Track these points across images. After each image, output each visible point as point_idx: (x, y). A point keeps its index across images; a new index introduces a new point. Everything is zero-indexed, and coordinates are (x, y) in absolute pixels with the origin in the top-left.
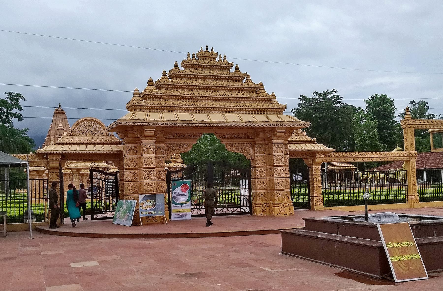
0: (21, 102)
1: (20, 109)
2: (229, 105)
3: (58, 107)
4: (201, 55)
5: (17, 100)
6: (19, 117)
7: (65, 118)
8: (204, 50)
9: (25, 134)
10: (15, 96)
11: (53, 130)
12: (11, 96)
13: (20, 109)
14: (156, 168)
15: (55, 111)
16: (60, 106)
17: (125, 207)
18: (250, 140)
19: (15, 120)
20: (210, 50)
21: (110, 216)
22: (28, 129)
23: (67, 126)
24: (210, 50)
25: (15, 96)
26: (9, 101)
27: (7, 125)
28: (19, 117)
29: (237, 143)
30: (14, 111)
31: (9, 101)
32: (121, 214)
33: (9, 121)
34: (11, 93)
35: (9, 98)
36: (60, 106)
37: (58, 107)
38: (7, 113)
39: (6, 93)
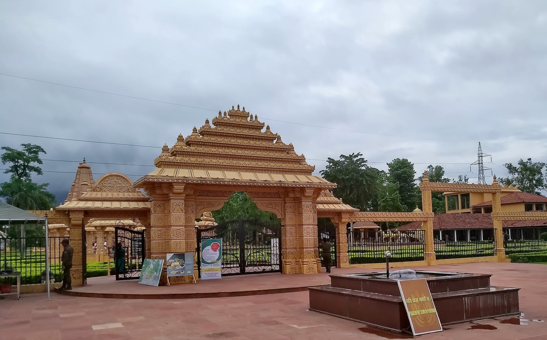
0: (41, 155)
1: (40, 162)
2: (260, 164)
4: (233, 114)
5: (36, 152)
6: (38, 171)
7: (90, 174)
8: (236, 109)
10: (33, 148)
11: (76, 185)
13: (40, 162)
14: (185, 226)
15: (79, 165)
16: (84, 161)
17: (152, 266)
18: (280, 199)
19: (33, 175)
20: (241, 110)
21: (136, 276)
22: (48, 184)
24: (241, 110)
25: (33, 148)
26: (27, 154)
27: (23, 179)
28: (38, 171)
29: (268, 202)
30: (32, 164)
31: (27, 154)
32: (147, 273)
33: (26, 175)
35: (27, 150)
36: (84, 161)
38: (24, 166)
39: (23, 145)
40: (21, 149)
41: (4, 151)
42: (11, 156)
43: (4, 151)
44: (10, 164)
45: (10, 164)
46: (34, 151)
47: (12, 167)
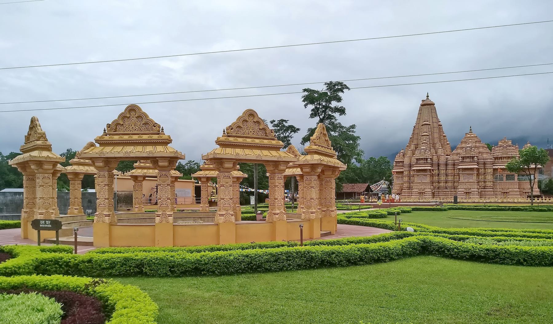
3: (425, 98)
6: (342, 111)
9: (353, 132)
12: (331, 86)
15: (421, 102)
16: (428, 96)
19: (336, 115)
22: (354, 125)
23: (435, 120)
25: (334, 86)
28: (342, 111)
30: (334, 104)
31: (329, 94)
33: (330, 117)
34: (331, 83)
36: (428, 96)
37: (425, 98)
39: (326, 84)
40: (322, 88)
41: (306, 93)
42: (311, 97)
43: (306, 93)
44: (311, 107)
45: (311, 107)
46: (336, 89)
47: (313, 110)
